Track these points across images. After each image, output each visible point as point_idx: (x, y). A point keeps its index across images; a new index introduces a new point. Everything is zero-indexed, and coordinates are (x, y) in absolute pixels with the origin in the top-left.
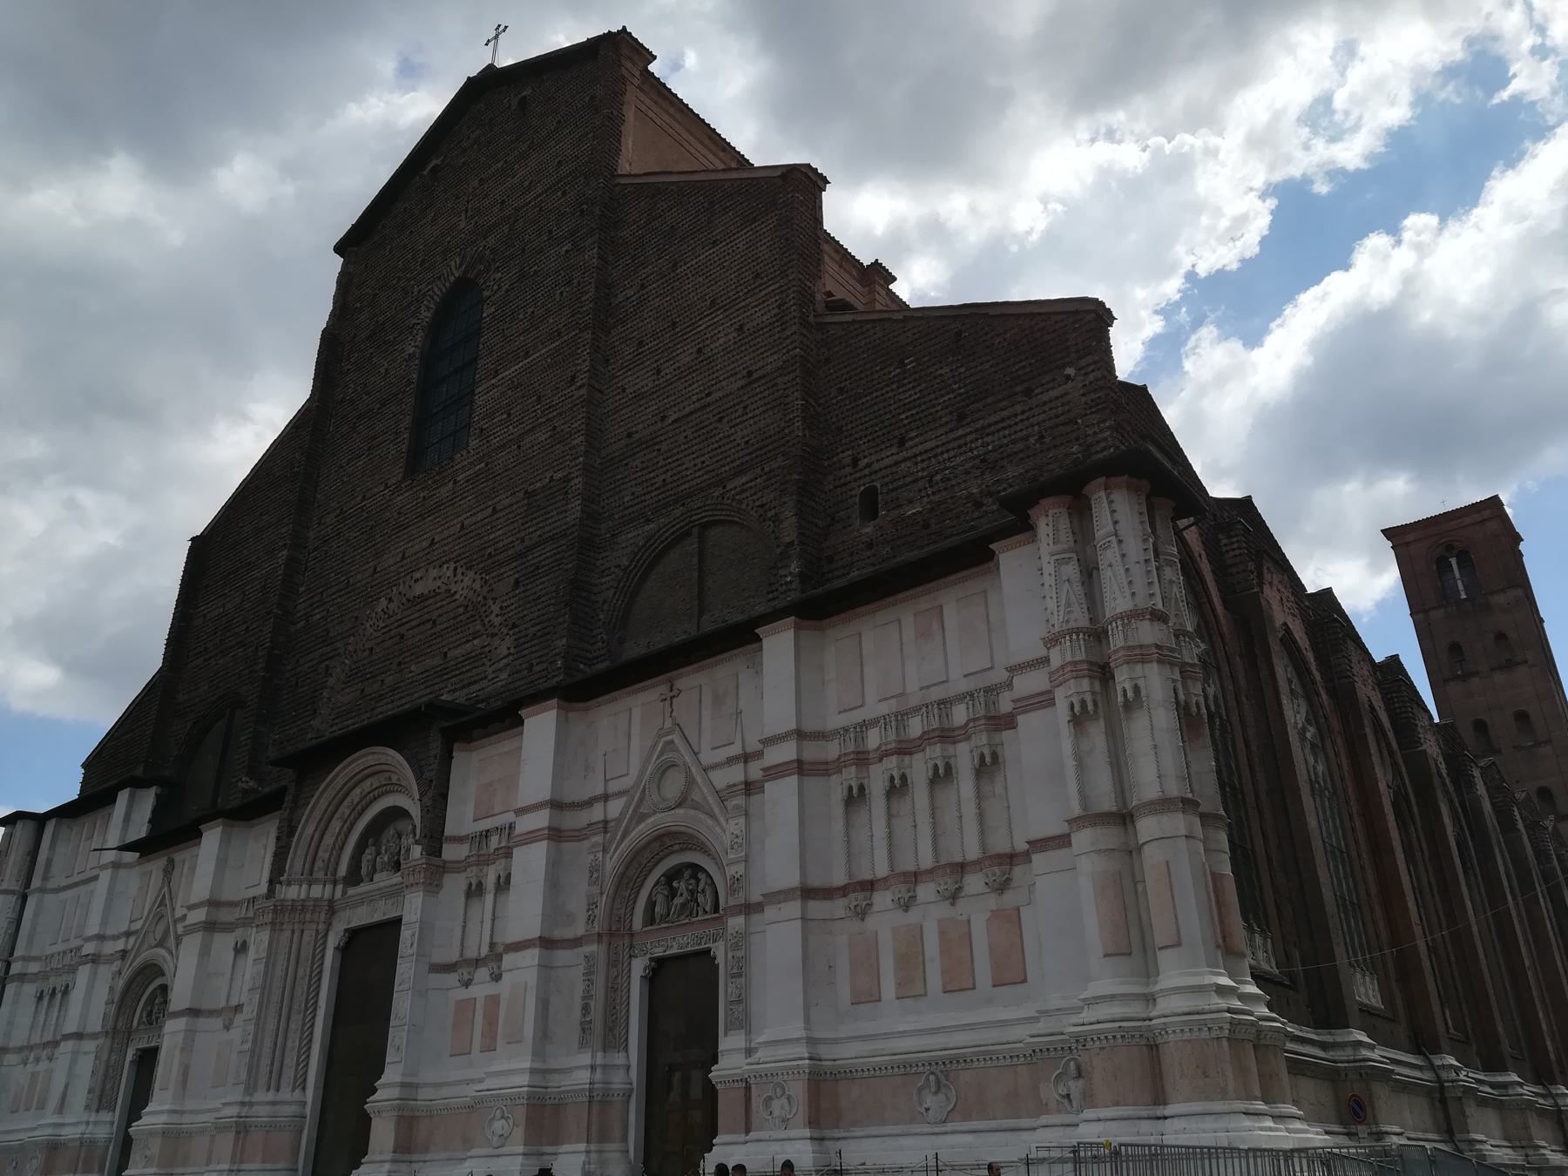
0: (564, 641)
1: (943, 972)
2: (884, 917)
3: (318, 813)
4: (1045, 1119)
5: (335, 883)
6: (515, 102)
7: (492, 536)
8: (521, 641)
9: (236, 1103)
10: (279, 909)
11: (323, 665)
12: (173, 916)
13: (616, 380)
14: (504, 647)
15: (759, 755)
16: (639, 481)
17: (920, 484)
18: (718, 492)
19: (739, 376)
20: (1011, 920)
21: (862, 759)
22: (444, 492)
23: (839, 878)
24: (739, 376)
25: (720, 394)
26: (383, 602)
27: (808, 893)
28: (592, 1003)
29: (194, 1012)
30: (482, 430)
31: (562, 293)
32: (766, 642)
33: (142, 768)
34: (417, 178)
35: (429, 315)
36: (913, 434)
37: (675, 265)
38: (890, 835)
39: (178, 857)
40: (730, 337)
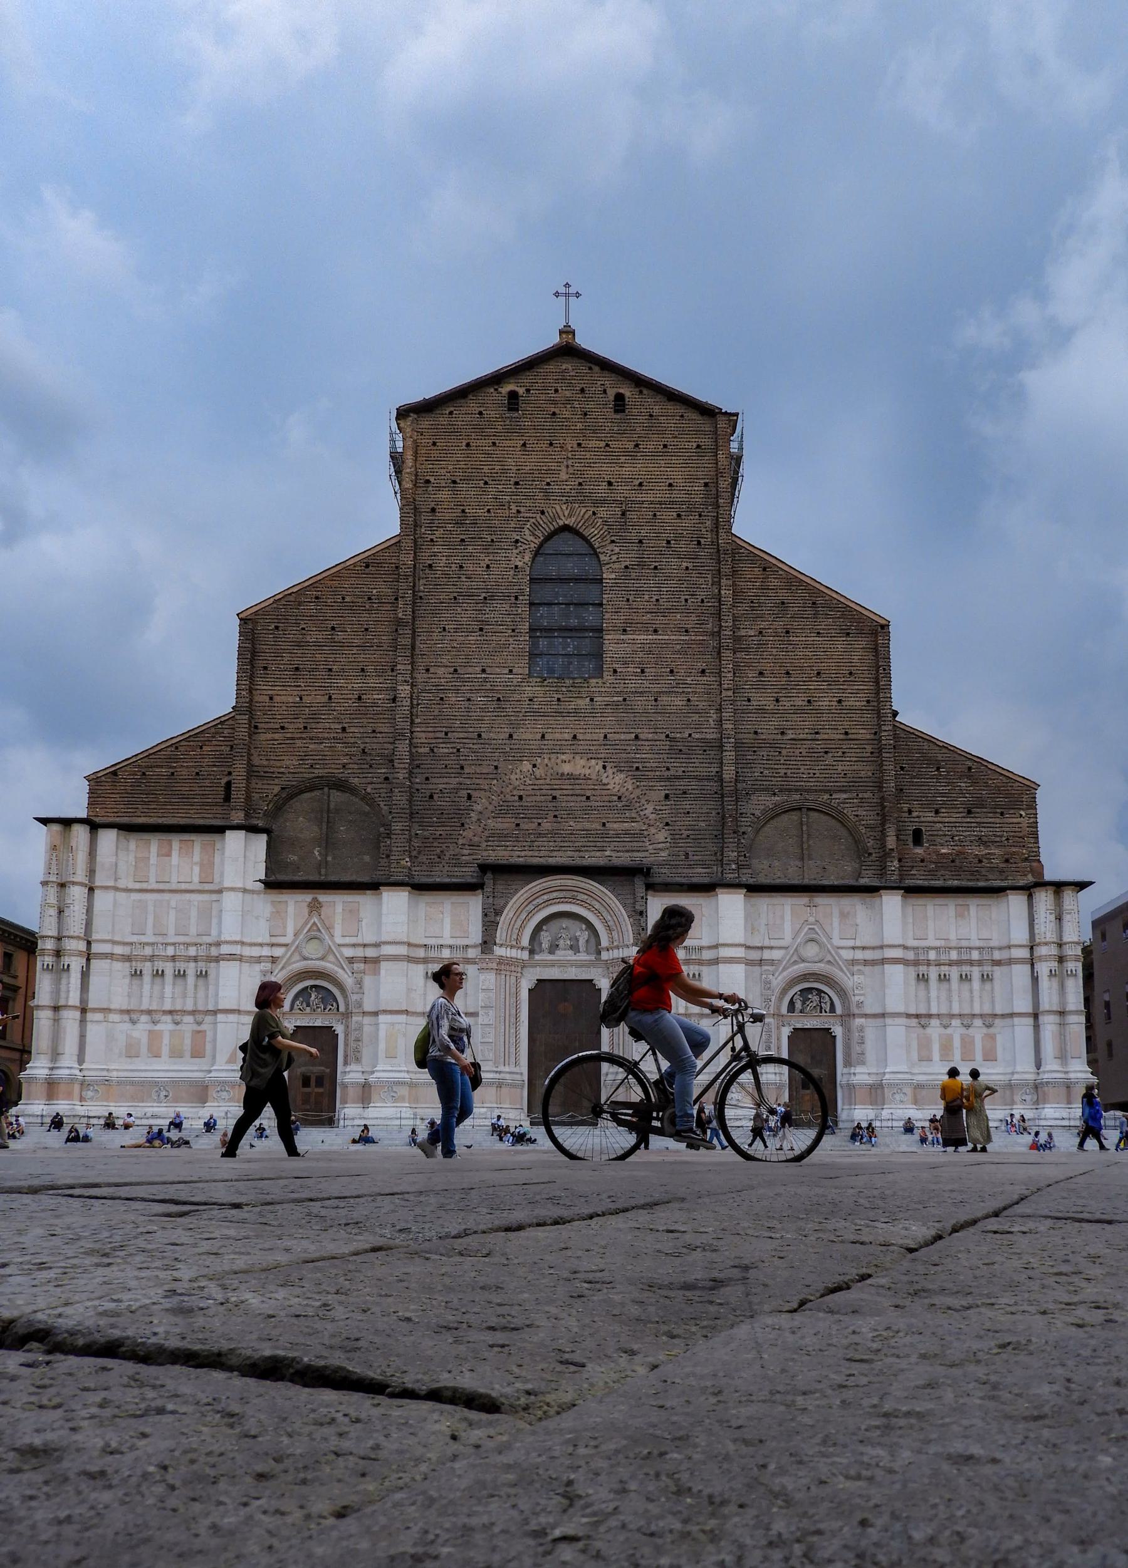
0: (736, 854)
1: (962, 1053)
2: (935, 1029)
3: (516, 906)
4: (1015, 1107)
5: (523, 949)
6: (611, 393)
7: (638, 756)
8: (677, 836)
9: (494, 1072)
10: (502, 961)
11: (465, 792)
12: (334, 943)
13: (741, 691)
14: (662, 836)
15: (874, 948)
16: (765, 766)
17: (948, 838)
18: (826, 796)
19: (839, 731)
20: (993, 1038)
21: (928, 963)
22: (584, 703)
23: (913, 1011)
24: (839, 731)
25: (826, 737)
26: (526, 766)
27: (908, 1016)
28: (772, 1046)
29: (406, 1012)
30: (615, 671)
31: (686, 600)
32: (884, 898)
33: (241, 814)
34: (492, 390)
35: (536, 541)
36: (943, 810)
37: (788, 632)
38: (938, 997)
39: (324, 897)
40: (832, 703)
